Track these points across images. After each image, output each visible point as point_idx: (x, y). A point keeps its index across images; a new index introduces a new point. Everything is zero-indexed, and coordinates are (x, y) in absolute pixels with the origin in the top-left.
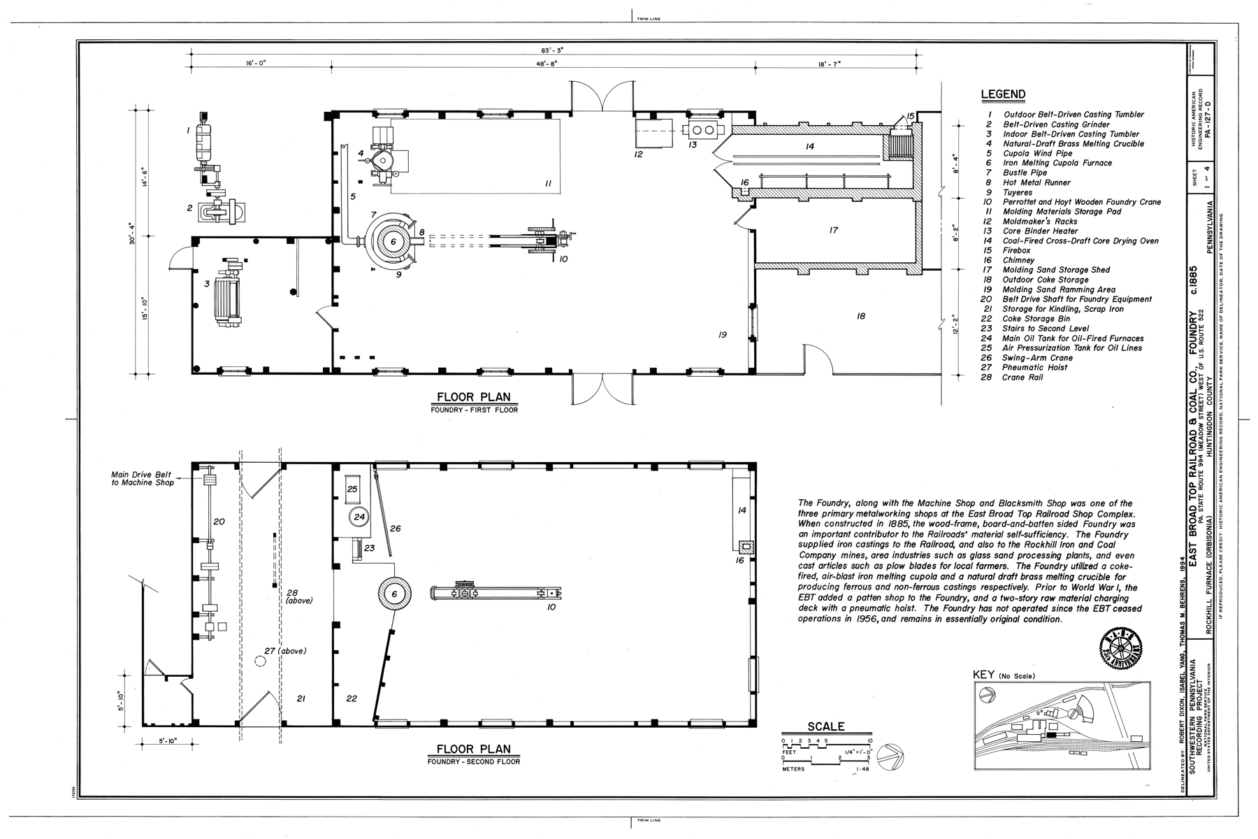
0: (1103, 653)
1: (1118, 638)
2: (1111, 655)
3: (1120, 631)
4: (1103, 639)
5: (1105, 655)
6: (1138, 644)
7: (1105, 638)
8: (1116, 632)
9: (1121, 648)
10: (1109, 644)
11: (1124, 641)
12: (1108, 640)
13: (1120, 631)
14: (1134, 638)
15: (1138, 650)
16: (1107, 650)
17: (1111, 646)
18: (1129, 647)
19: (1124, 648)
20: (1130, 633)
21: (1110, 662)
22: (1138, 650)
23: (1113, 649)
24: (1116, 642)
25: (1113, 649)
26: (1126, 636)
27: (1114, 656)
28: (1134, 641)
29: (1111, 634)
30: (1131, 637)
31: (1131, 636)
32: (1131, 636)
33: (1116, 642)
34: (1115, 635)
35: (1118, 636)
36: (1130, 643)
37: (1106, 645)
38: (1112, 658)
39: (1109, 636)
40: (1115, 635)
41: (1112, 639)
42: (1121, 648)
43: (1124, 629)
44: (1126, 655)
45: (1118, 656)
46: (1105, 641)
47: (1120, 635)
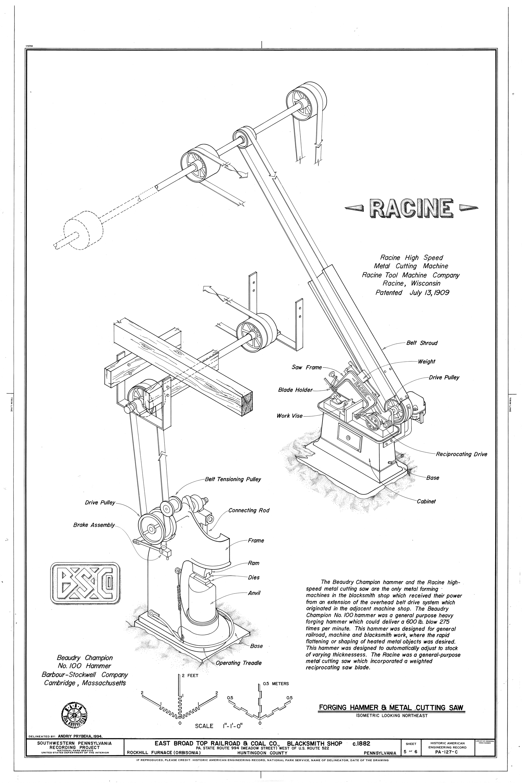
0: (63, 718)
1: (73, 709)
2: (68, 719)
3: (74, 704)
4: (63, 709)
5: (65, 719)
6: (85, 713)
7: (65, 708)
8: (72, 705)
9: (74, 715)
10: (67, 712)
11: (76, 711)
12: (67, 710)
13: (74, 704)
14: (83, 709)
15: (85, 716)
16: (66, 716)
17: (68, 714)
18: (79, 715)
19: (73, 714)
20: (80, 706)
21: (67, 723)
22: (85, 716)
23: (70, 716)
24: (72, 711)
25: (70, 716)
26: (78, 708)
27: (70, 720)
28: (83, 711)
29: (69, 706)
30: (80, 709)
31: (81, 708)
32: (81, 708)
33: (72, 711)
34: (71, 707)
35: (73, 707)
36: (80, 712)
37: (65, 713)
38: (69, 721)
39: (67, 708)
40: (71, 707)
41: (69, 709)
42: (74, 715)
43: (76, 704)
44: (77, 719)
45: (73, 720)
46: (65, 711)
47: (74, 707)
